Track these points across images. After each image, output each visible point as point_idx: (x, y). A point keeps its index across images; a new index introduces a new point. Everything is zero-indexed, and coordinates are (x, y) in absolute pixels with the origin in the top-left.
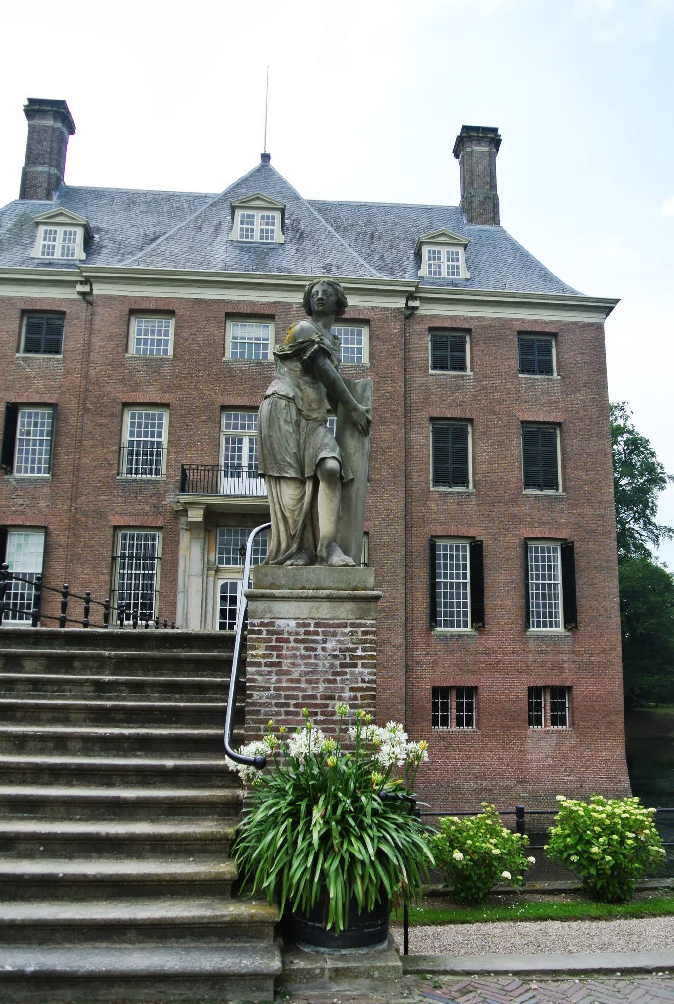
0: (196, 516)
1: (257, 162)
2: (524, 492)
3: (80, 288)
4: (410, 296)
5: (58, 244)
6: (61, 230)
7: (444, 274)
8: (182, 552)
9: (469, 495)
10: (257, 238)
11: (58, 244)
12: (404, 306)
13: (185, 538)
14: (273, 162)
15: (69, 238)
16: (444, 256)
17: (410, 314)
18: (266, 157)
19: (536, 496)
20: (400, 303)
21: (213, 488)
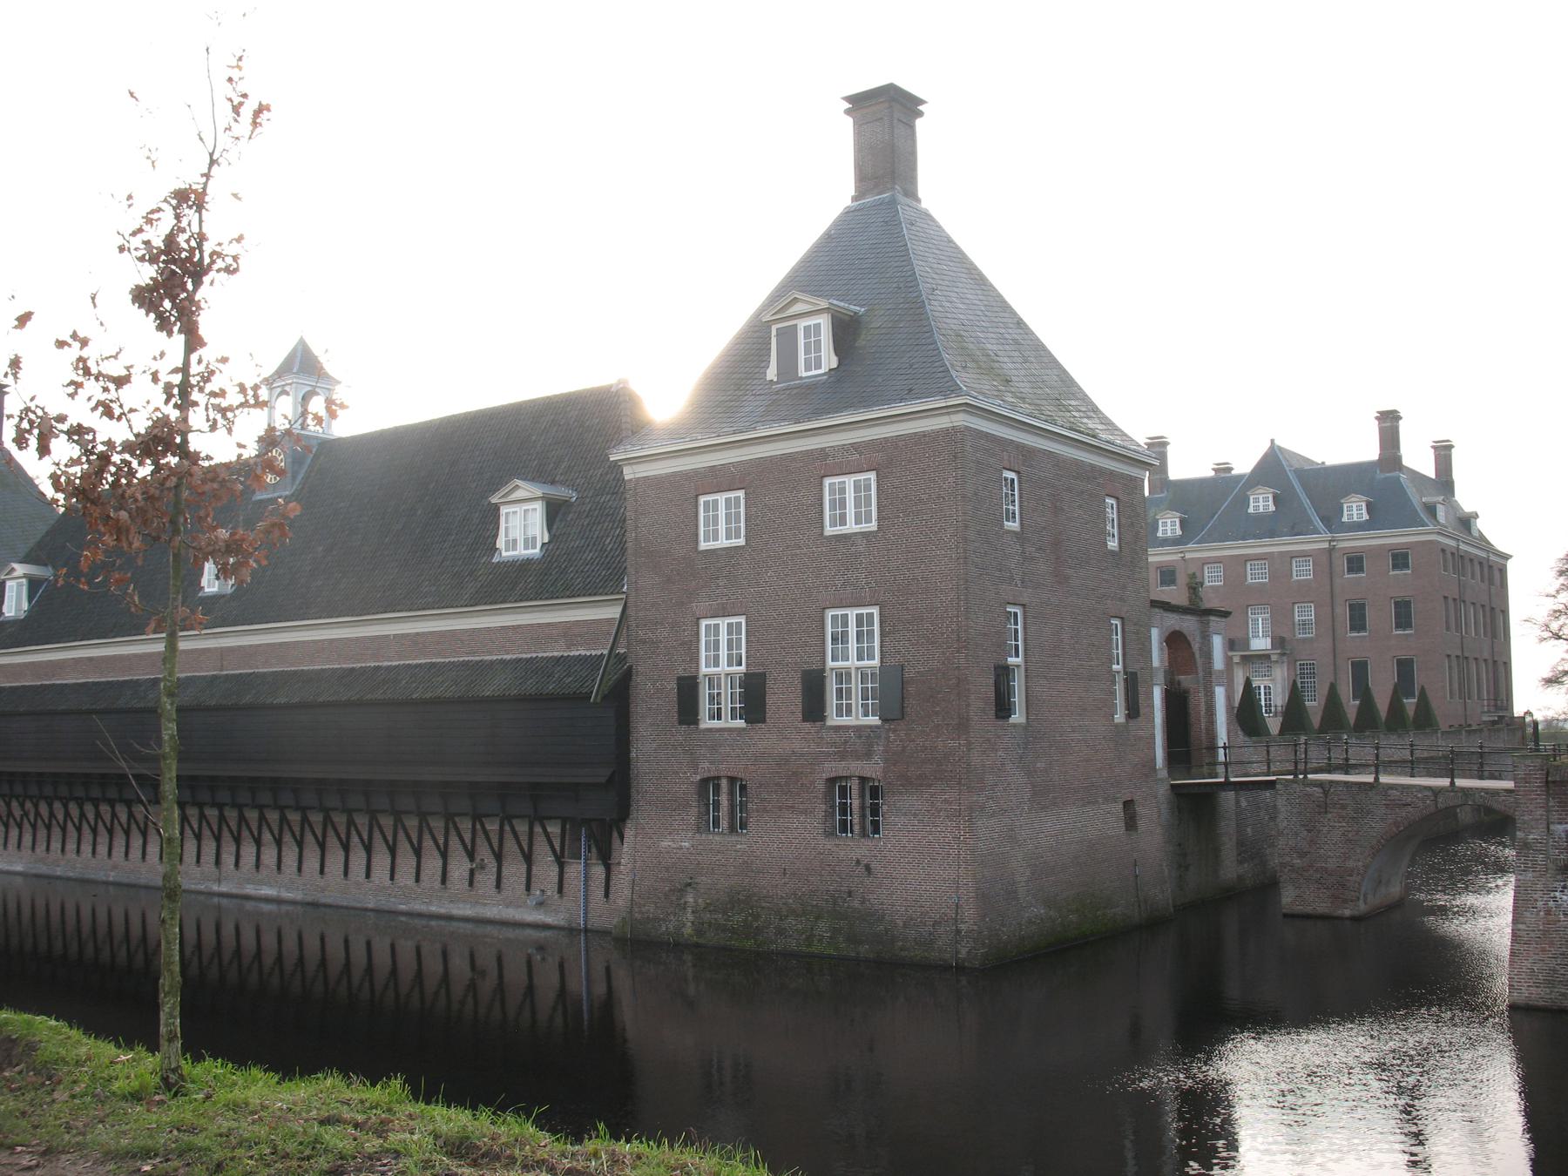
0: (1236, 660)
1: (1268, 444)
2: (1395, 632)
3: (1180, 555)
4: (1330, 541)
5: (1169, 528)
6: (1169, 521)
7: (1355, 519)
8: (1235, 674)
9: (1365, 637)
10: (1261, 510)
11: (1169, 528)
12: (1327, 546)
13: (1235, 667)
14: (1277, 443)
15: (1173, 524)
16: (1355, 509)
17: (1331, 550)
18: (1272, 441)
19: (1400, 634)
20: (1326, 545)
21: (1246, 643)
